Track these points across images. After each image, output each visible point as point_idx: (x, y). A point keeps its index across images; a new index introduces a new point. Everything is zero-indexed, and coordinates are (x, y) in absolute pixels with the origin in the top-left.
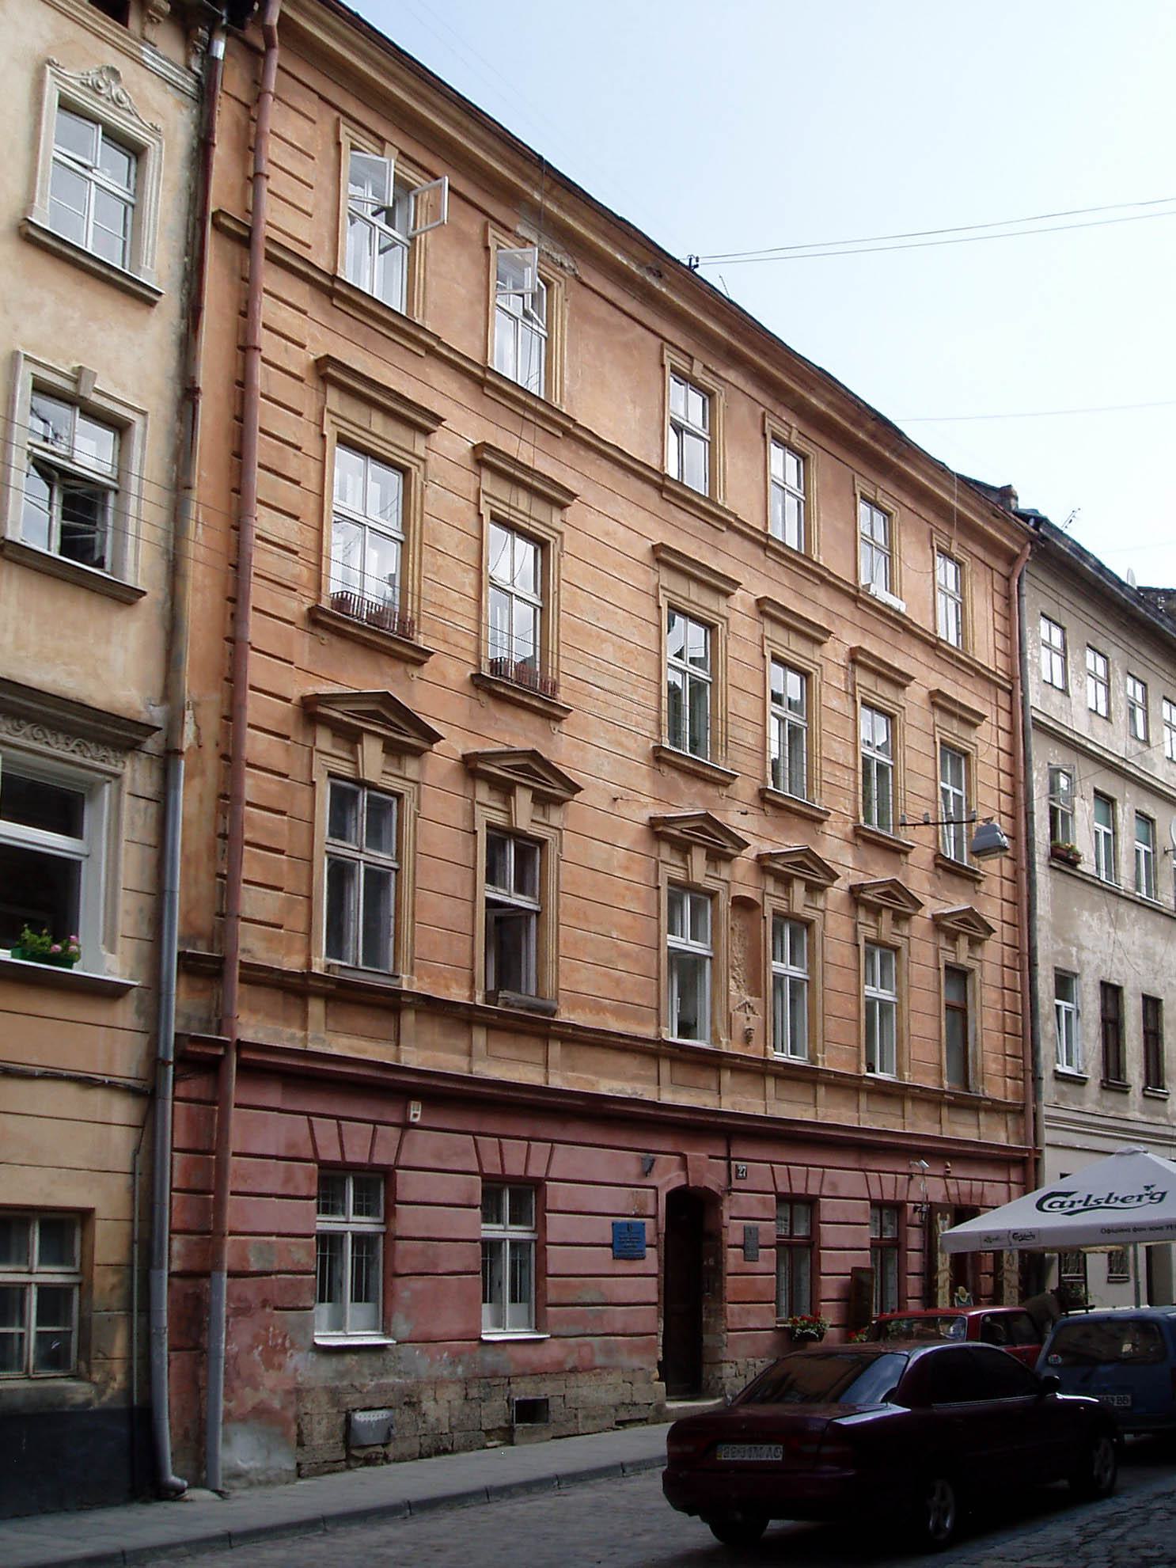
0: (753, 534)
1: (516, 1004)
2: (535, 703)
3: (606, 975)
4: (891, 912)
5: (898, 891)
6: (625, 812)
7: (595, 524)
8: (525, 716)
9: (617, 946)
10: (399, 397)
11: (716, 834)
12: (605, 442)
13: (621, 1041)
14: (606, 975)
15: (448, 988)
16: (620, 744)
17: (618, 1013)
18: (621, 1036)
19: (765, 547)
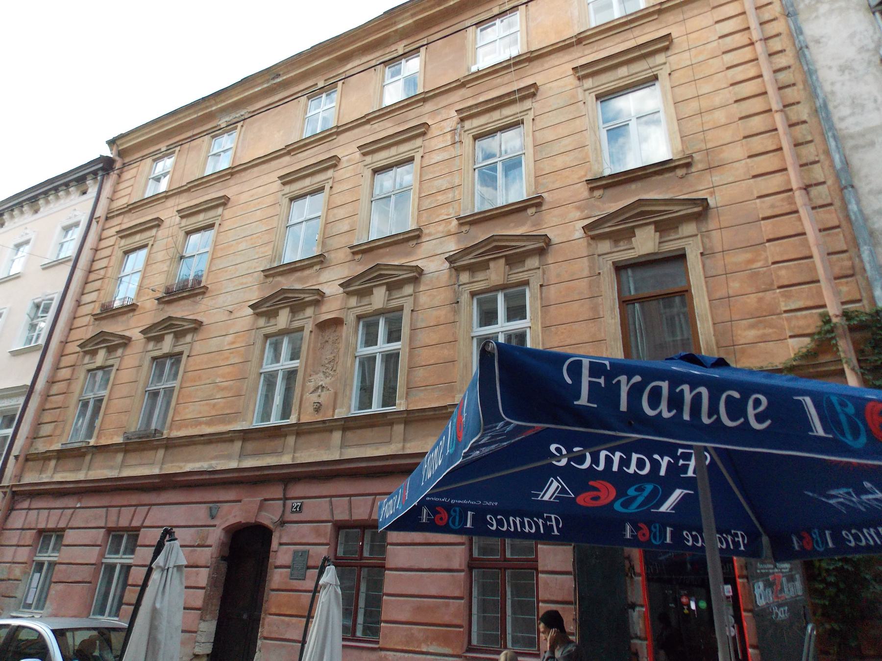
0: (355, 124)
1: (133, 437)
2: (184, 294)
3: (207, 404)
4: (503, 261)
5: (507, 240)
6: (238, 315)
7: (244, 198)
8: (182, 302)
9: (218, 386)
10: (141, 224)
11: (296, 295)
12: (250, 162)
13: (202, 438)
14: (207, 404)
15: (112, 439)
16: (242, 284)
17: (209, 423)
18: (202, 436)
19: (368, 122)
